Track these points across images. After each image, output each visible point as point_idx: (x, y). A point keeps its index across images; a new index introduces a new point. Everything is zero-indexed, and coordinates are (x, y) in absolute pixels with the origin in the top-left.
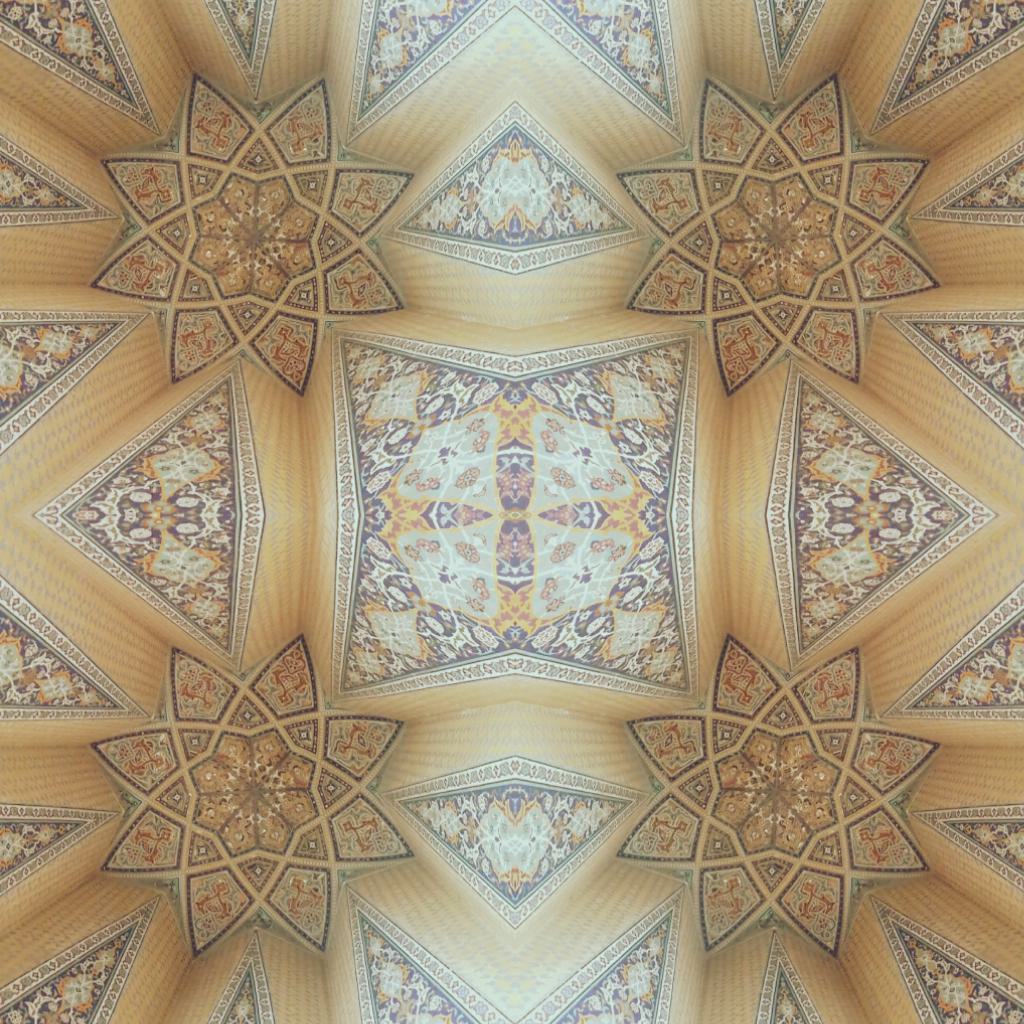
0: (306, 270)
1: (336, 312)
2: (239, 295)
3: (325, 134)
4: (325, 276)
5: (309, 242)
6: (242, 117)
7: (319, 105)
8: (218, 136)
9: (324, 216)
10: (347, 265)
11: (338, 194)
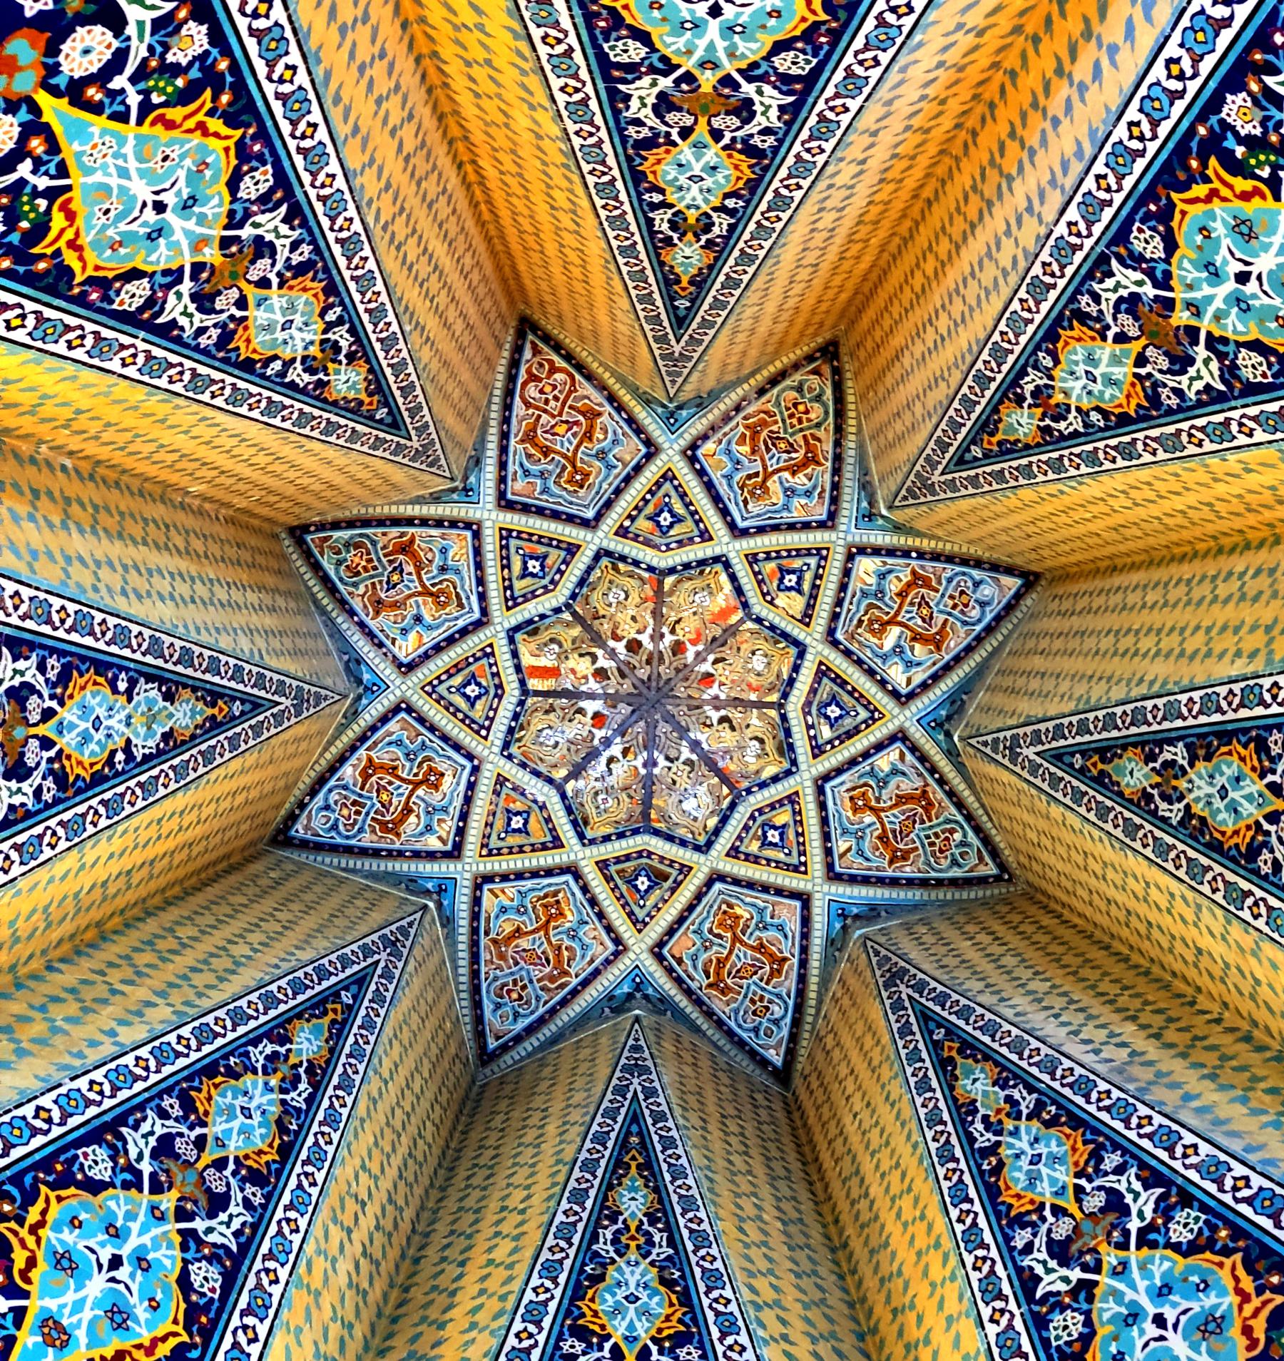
0: (530, 627)
1: (453, 524)
2: (687, 566)
3: (483, 941)
4: (484, 611)
5: (525, 692)
6: (679, 981)
7: (498, 1006)
8: (736, 939)
9: (488, 750)
10: (430, 638)
11: (458, 803)
